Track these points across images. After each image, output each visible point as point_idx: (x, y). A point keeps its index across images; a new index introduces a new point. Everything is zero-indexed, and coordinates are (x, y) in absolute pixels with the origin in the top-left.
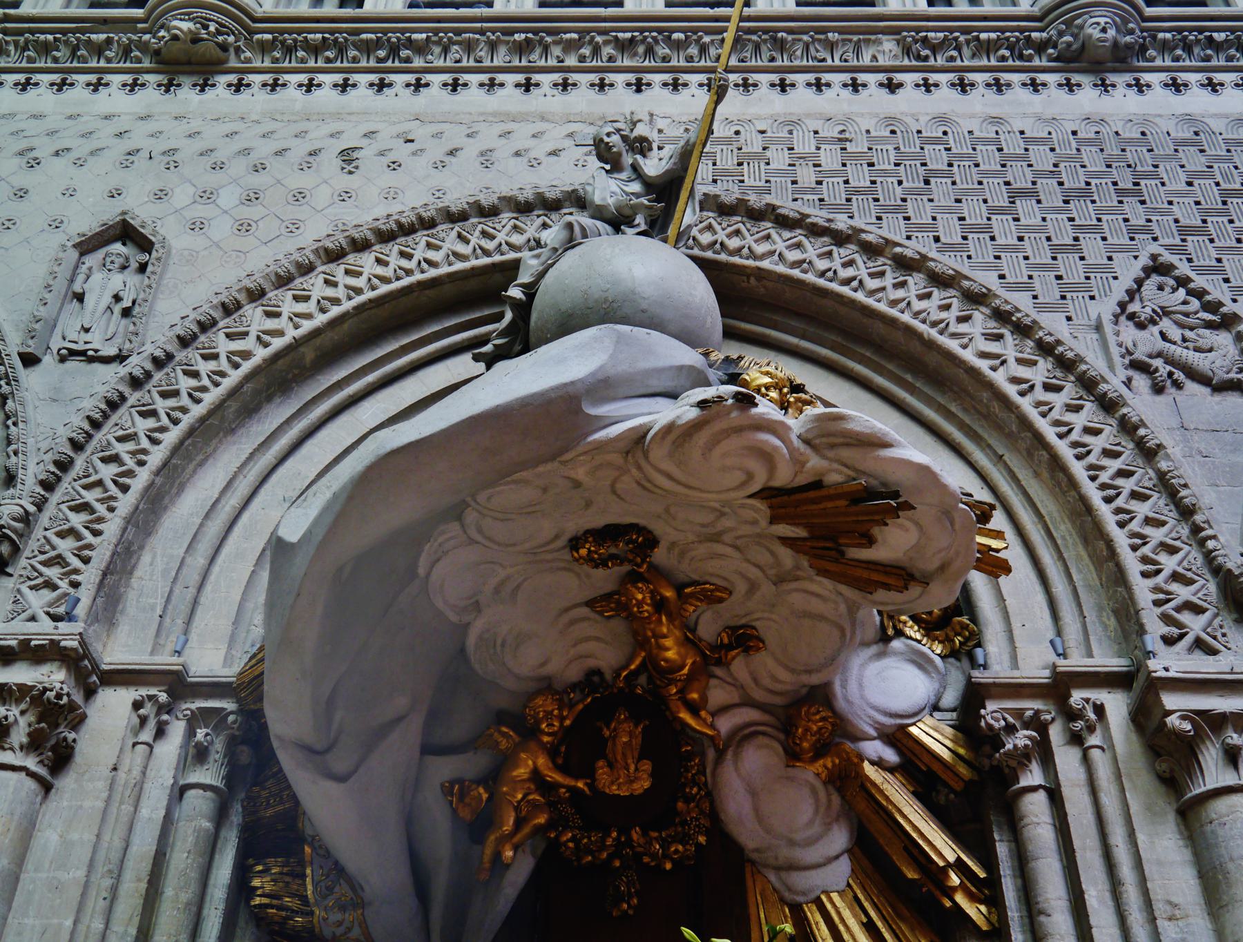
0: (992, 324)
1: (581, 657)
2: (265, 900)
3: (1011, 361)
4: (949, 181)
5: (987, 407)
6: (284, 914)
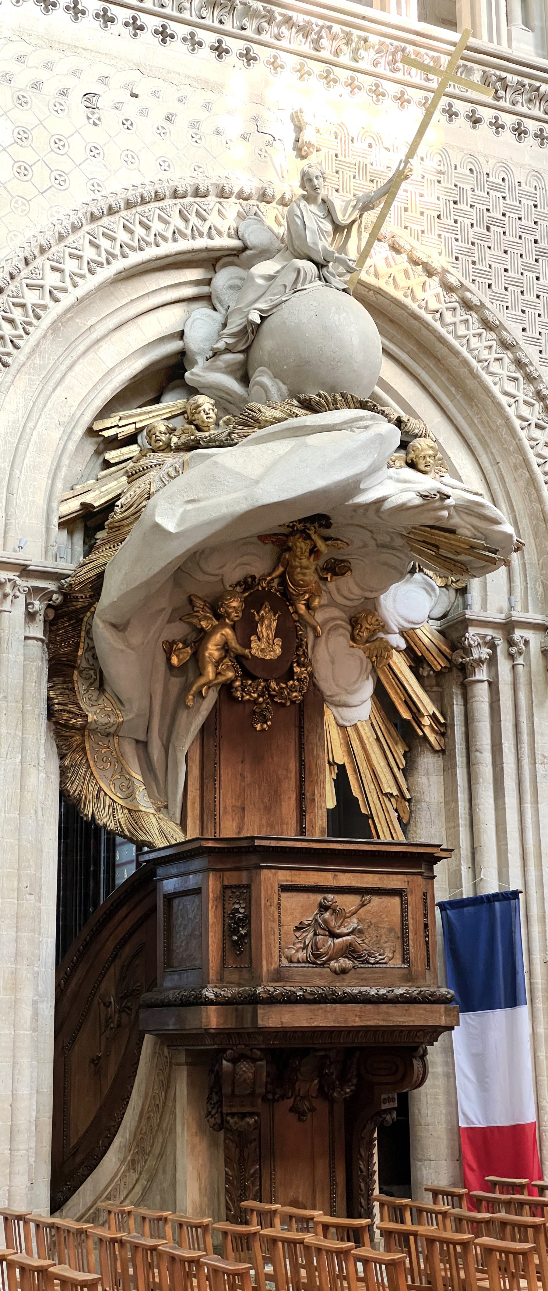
0: (513, 367)
1: (244, 564)
2: (61, 707)
3: (521, 402)
4: (502, 230)
5: (498, 427)
6: (70, 716)
